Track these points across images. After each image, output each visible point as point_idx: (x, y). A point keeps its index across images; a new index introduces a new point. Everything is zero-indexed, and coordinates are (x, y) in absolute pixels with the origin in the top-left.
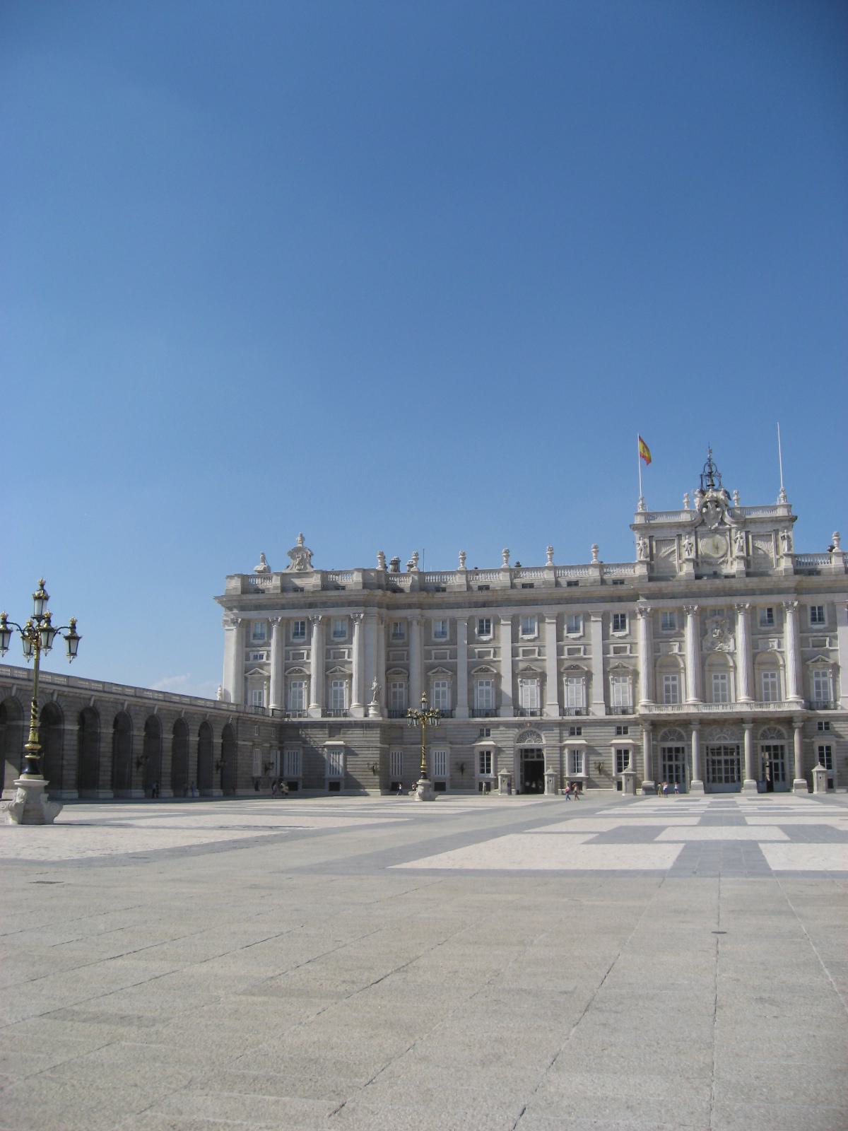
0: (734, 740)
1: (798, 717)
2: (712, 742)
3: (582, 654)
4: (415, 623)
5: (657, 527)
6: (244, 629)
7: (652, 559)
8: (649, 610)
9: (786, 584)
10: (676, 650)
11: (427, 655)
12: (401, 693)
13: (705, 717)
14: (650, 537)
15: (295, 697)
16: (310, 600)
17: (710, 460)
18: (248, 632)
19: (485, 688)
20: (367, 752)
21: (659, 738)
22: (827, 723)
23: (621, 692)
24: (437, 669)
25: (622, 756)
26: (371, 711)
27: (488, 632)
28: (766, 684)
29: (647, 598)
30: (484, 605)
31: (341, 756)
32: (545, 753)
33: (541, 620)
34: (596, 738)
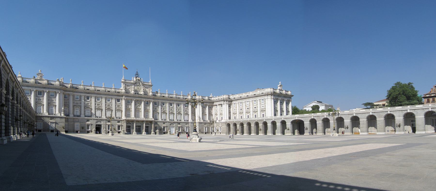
3: (110, 106)
4: (71, 95)
7: (125, 89)
8: (126, 99)
9: (151, 97)
10: (130, 107)
11: (74, 103)
12: (67, 111)
15: (39, 109)
19: (88, 111)
22: (157, 123)
23: (118, 114)
25: (119, 127)
26: (62, 114)
27: (89, 99)
28: (146, 115)
30: (88, 93)
31: (54, 124)
32: (102, 125)
33: (102, 98)
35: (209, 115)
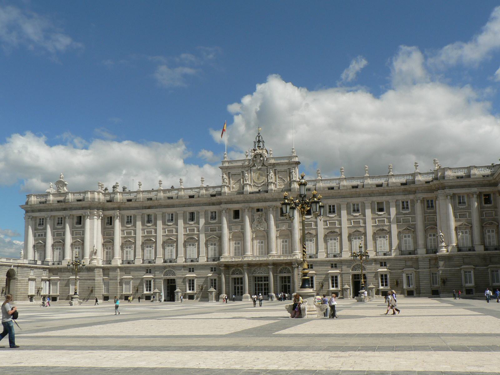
0: (266, 274)
1: (294, 262)
2: (256, 275)
5: (232, 168)
6: (34, 222)
13: (250, 262)
14: (229, 173)
16: (64, 207)
17: (259, 134)
18: (36, 223)
20: (89, 282)
21: (231, 273)
24: (211, 237)
29: (226, 203)
30: (149, 208)
34: (200, 273)
35: (482, 227)
